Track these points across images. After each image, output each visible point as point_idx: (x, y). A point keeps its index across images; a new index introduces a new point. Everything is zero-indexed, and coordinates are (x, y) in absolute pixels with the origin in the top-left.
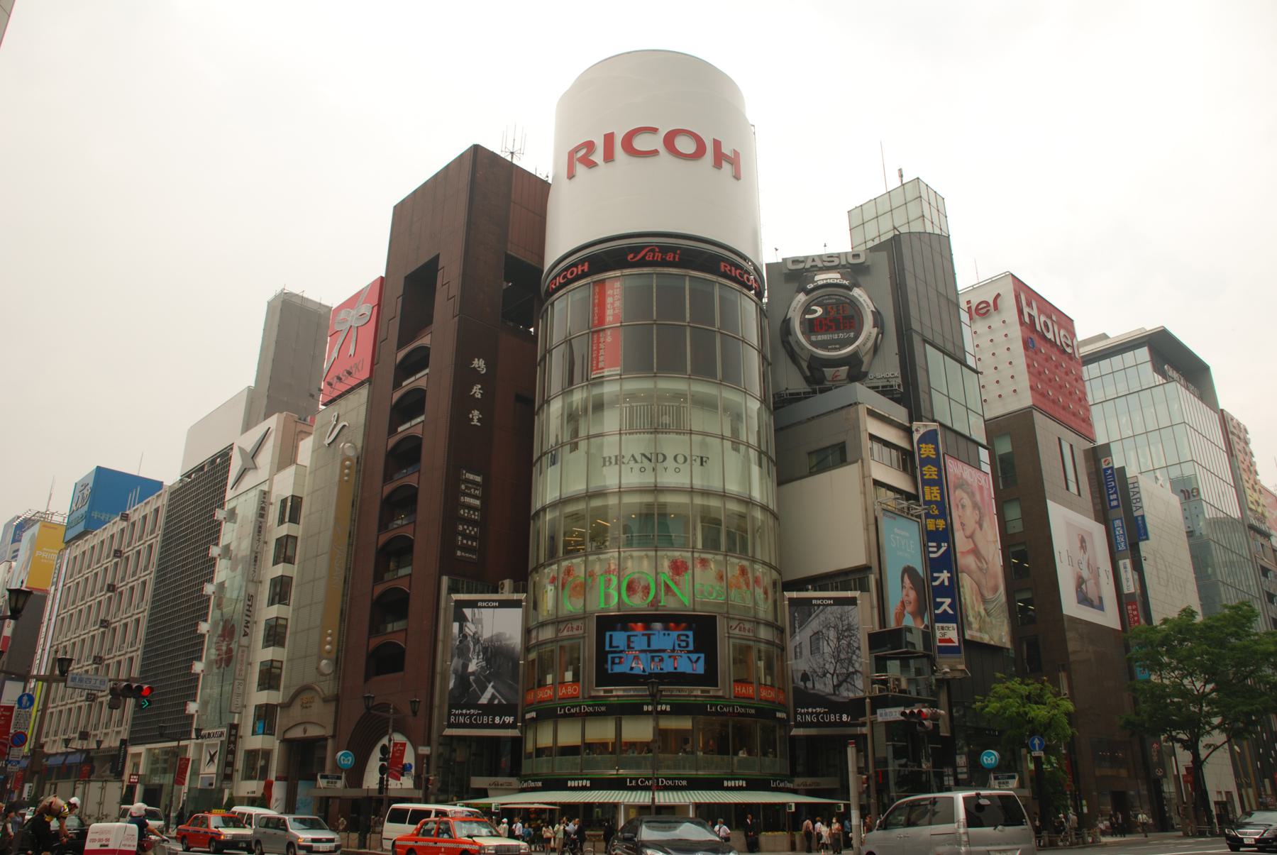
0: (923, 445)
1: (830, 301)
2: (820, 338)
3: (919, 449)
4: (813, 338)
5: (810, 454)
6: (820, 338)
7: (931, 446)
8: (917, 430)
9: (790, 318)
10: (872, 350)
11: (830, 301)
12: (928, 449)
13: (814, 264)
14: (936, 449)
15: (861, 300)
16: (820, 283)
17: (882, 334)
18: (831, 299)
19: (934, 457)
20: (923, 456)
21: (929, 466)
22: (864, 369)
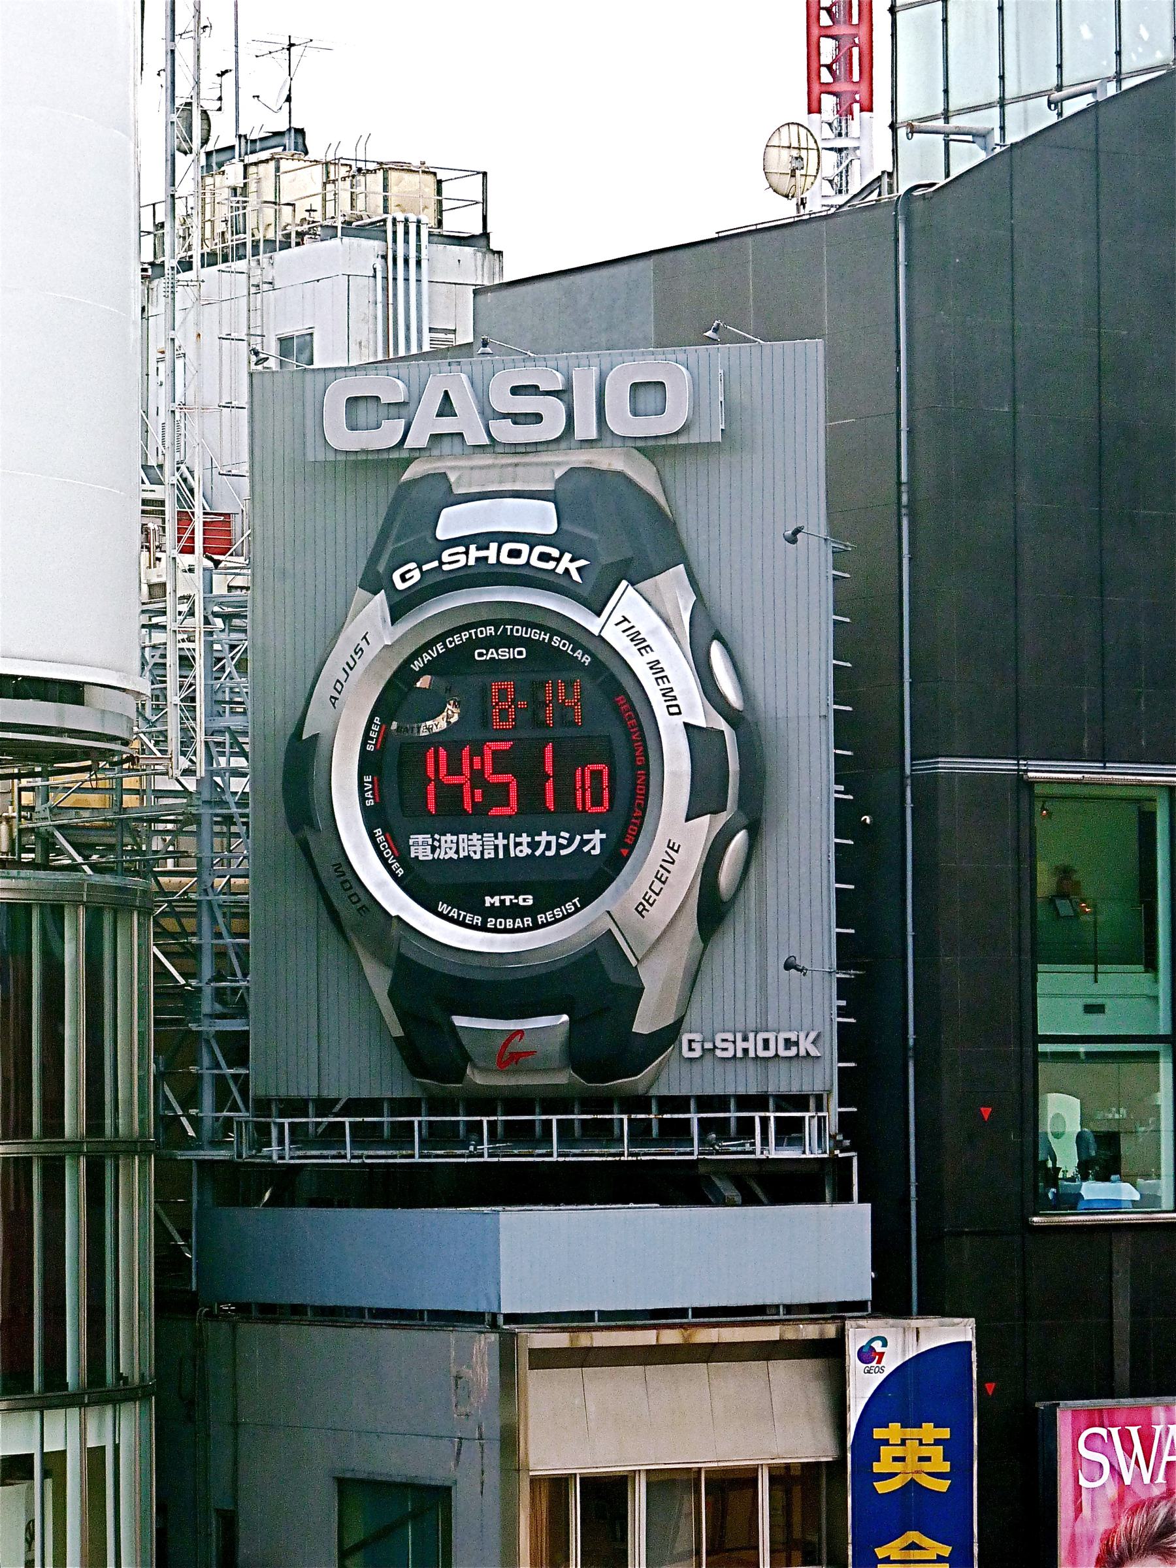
0: (894, 1431)
1: (504, 654)
2: (451, 846)
3: (868, 1449)
4: (420, 847)
5: (346, 1486)
6: (451, 846)
7: (929, 1431)
8: (867, 1355)
9: (316, 736)
10: (690, 925)
11: (504, 654)
12: (912, 1451)
13: (446, 425)
14: (954, 1450)
15: (639, 664)
16: (454, 560)
17: (755, 830)
18: (511, 642)
19: (942, 1486)
20: (882, 1487)
21: (914, 1536)
22: (644, 1024)
